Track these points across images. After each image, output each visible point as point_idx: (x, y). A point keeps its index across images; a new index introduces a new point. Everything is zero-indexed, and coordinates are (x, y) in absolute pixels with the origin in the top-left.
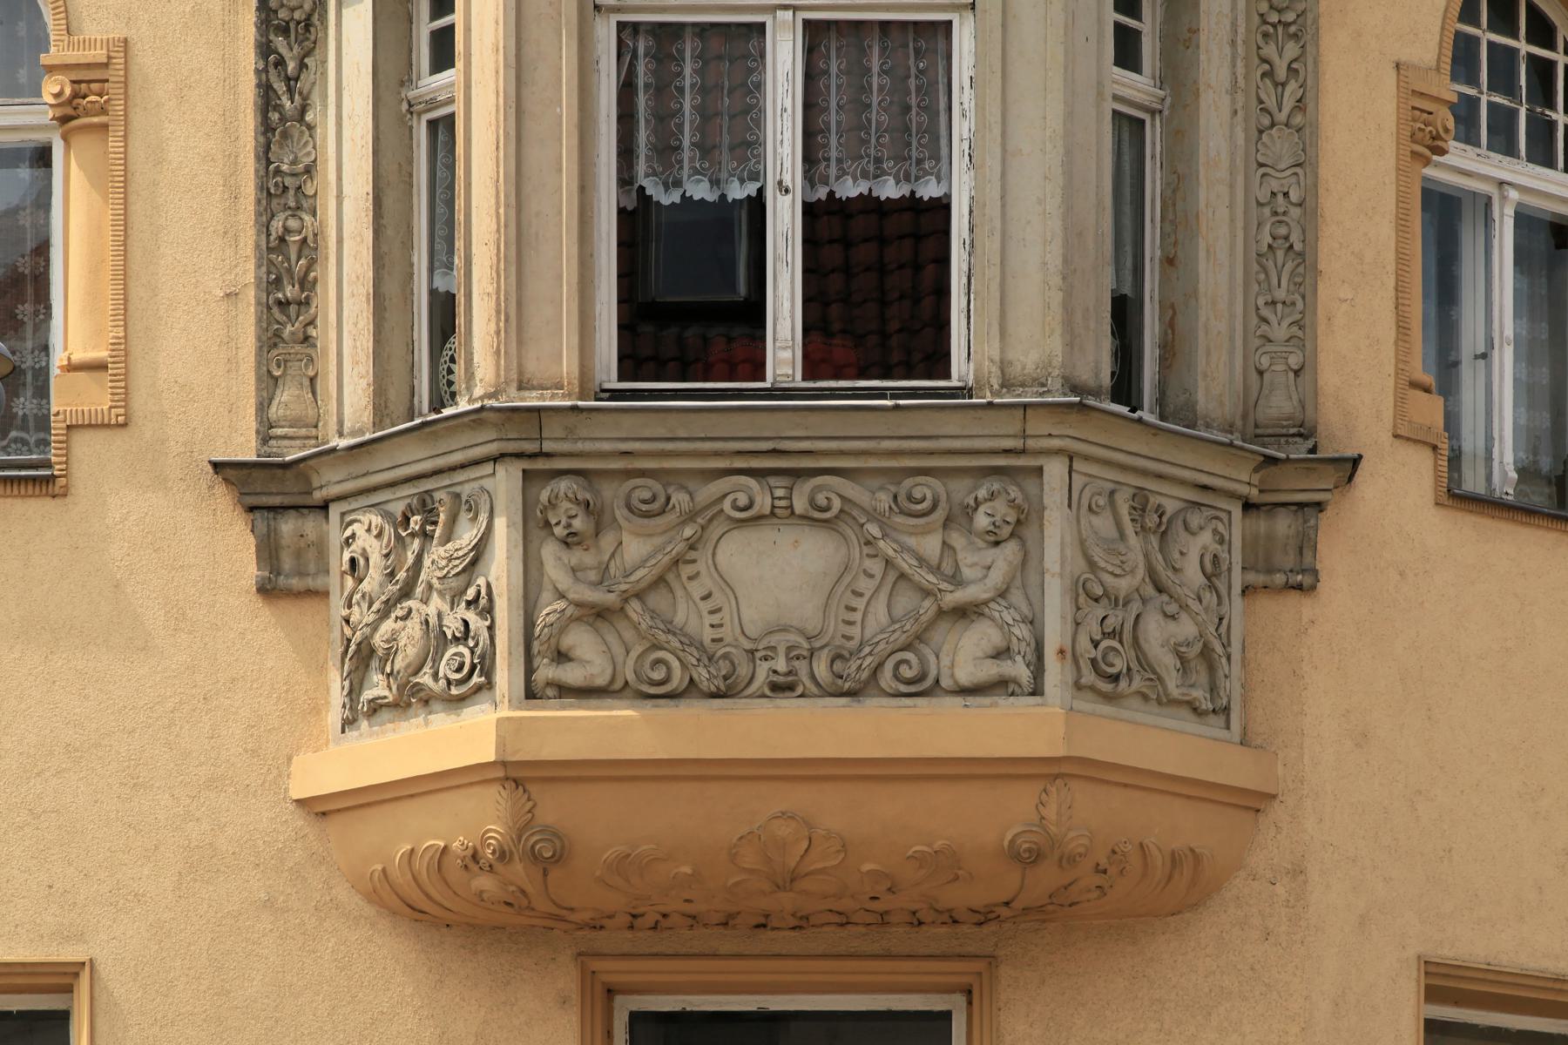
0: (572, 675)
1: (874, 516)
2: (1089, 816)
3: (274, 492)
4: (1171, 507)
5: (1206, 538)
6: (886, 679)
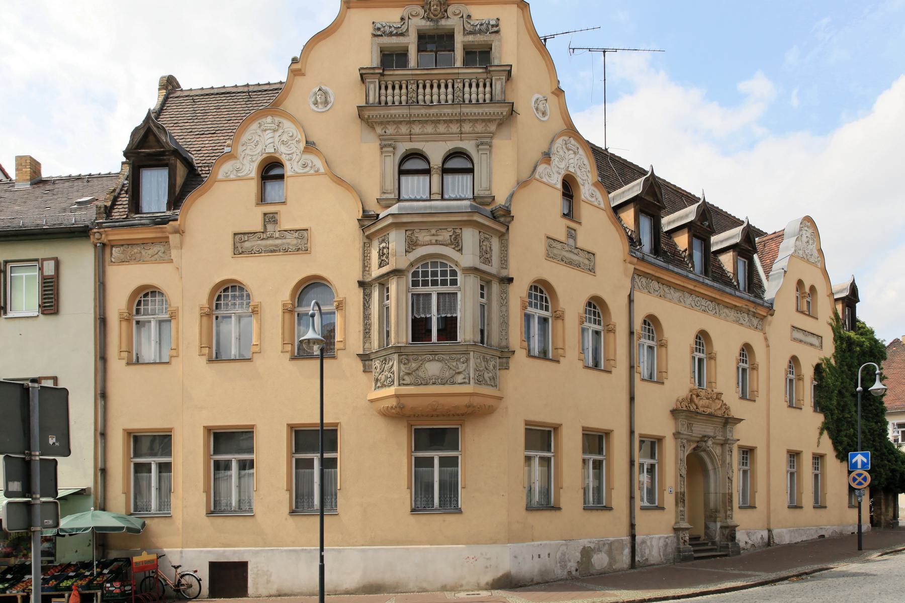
0: (405, 382)
2: (476, 401)
3: (365, 358)
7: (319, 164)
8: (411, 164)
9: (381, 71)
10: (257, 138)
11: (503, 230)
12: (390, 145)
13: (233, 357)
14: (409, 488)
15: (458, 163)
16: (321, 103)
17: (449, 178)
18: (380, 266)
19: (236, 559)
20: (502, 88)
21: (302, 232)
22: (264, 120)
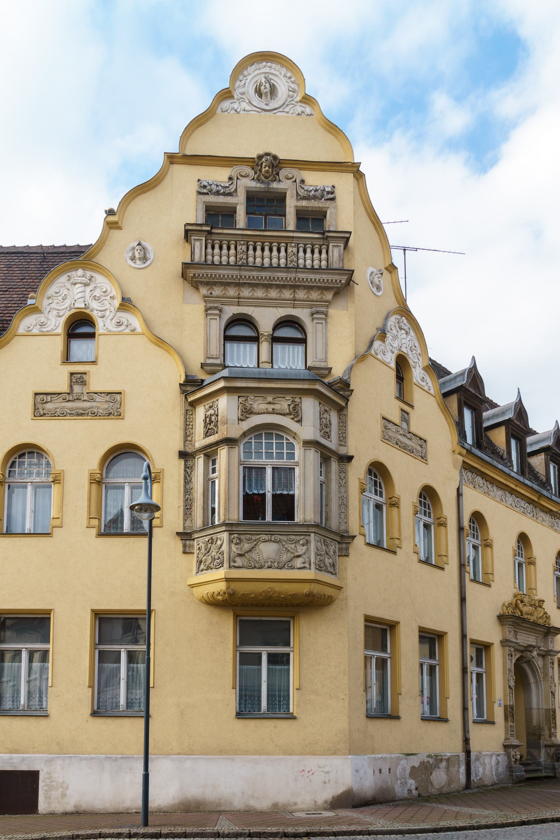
0: (236, 565)
1: (284, 541)
2: (316, 589)
3: (185, 536)
4: (329, 542)
5: (333, 547)
6: (286, 566)
7: (136, 322)
8: (240, 329)
9: (209, 229)
10: (66, 292)
11: (343, 404)
12: (216, 308)
13: (26, 532)
14: (234, 688)
15: (290, 332)
16: (140, 259)
17: (279, 348)
18: (206, 435)
19: (24, 768)
20: (340, 256)
21: (114, 396)
22: (74, 273)
